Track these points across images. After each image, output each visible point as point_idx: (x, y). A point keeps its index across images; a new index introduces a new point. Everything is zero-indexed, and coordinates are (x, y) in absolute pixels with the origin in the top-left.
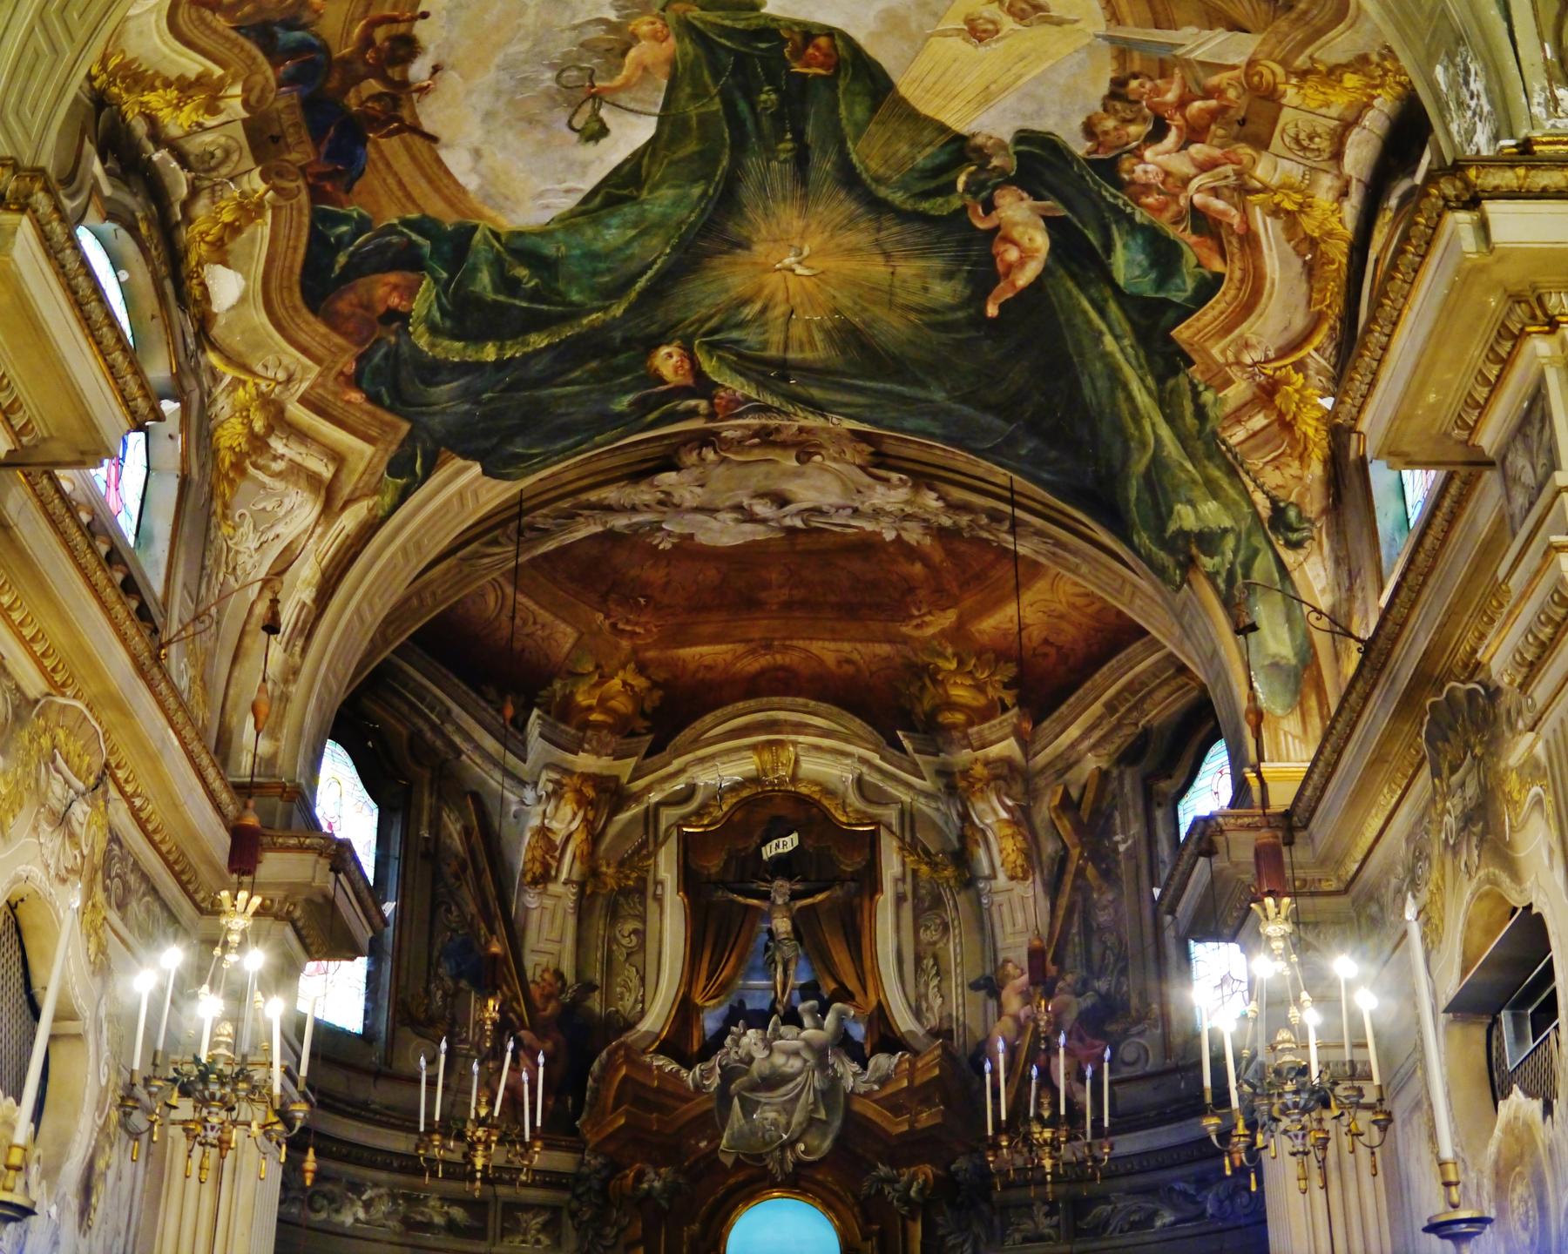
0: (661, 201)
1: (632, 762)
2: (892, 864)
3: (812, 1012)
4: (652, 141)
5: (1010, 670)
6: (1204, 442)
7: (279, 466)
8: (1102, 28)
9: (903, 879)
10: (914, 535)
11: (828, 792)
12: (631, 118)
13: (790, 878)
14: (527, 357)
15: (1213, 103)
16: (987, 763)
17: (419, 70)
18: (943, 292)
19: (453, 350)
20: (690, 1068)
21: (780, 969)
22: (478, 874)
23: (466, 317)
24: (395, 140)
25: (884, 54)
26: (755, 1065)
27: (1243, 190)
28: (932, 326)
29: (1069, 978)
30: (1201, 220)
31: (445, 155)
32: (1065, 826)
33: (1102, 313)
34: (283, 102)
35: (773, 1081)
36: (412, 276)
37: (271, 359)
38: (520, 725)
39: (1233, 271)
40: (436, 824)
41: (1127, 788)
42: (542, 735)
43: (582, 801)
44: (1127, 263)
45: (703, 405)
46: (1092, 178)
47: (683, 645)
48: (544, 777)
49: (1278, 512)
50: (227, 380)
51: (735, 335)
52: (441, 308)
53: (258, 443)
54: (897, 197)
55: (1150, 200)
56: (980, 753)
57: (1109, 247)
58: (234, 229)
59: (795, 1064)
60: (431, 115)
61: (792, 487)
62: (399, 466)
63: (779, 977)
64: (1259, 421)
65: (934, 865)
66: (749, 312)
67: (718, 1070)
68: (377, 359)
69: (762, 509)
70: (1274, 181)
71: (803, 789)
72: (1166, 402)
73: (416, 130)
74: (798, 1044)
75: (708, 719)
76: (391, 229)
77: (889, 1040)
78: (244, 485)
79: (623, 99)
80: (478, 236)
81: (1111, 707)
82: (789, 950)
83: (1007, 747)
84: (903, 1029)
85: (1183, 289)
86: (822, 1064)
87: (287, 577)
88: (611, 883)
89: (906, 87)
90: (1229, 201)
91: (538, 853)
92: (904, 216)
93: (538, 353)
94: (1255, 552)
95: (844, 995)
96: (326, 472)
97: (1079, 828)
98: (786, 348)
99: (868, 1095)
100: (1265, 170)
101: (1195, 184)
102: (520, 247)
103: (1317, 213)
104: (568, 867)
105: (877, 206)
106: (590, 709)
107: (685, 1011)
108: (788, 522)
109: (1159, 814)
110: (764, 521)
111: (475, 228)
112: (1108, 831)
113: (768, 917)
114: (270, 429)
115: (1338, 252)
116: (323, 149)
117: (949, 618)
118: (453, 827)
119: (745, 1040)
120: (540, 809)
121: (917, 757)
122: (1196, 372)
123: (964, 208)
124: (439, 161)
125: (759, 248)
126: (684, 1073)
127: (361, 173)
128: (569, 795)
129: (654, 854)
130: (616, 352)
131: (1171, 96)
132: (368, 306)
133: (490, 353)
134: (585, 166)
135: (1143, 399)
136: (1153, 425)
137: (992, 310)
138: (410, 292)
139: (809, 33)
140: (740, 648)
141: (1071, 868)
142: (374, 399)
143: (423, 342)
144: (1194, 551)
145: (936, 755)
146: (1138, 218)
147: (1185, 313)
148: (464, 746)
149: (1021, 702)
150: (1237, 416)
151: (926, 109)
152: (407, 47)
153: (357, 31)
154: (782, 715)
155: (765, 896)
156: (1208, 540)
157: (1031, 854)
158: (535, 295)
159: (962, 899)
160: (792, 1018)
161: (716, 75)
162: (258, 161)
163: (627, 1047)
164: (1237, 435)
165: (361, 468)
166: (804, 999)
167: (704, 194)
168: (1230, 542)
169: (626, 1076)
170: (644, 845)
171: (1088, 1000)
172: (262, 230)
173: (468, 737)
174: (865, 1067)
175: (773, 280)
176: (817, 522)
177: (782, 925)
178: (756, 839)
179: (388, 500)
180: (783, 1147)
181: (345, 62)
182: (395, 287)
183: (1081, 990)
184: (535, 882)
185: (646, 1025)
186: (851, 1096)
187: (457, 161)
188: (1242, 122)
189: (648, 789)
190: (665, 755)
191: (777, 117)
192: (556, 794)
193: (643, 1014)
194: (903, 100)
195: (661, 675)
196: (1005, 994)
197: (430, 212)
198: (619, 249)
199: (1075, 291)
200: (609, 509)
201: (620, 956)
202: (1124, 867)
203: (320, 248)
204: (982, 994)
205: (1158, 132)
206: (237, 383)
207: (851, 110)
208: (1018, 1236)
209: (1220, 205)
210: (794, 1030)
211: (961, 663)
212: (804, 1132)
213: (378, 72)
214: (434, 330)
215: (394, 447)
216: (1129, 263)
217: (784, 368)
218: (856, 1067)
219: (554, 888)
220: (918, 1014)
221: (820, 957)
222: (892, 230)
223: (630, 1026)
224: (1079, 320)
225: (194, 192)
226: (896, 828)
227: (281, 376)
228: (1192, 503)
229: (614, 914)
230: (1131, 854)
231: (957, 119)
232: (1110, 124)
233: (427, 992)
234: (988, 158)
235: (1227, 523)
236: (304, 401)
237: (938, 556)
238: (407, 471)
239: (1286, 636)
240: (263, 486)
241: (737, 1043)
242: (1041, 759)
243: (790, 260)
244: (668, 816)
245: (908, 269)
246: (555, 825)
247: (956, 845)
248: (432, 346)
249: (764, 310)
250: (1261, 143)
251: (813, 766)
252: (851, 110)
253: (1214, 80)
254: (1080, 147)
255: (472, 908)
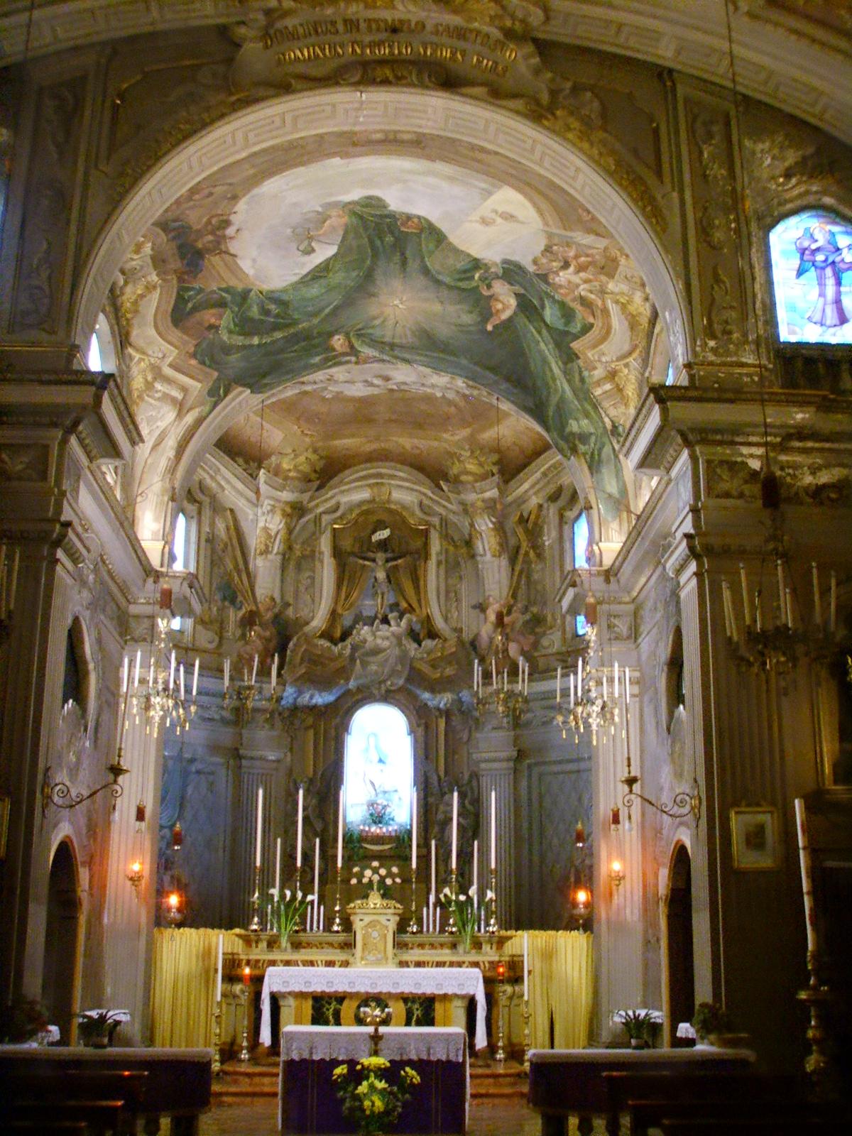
0: (337, 277)
1: (309, 494)
2: (436, 545)
3: (395, 618)
4: (335, 255)
5: (495, 457)
6: (583, 392)
7: (158, 395)
8: (542, 227)
9: (441, 553)
10: (451, 395)
11: (404, 507)
12: (327, 246)
13: (386, 551)
14: (273, 342)
15: (589, 259)
16: (483, 501)
17: (230, 231)
18: (468, 319)
19: (239, 340)
20: (336, 644)
21: (380, 596)
22: (233, 550)
23: (246, 326)
24: (217, 257)
25: (443, 226)
26: (367, 644)
27: (603, 292)
28: (462, 331)
29: (519, 605)
30: (583, 301)
31: (239, 262)
32: (520, 531)
33: (539, 333)
34: (169, 249)
35: (376, 651)
36: (221, 310)
37: (156, 349)
38: (254, 477)
39: (598, 324)
40: (212, 525)
41: (551, 514)
42: (265, 482)
43: (285, 515)
44: (550, 314)
45: (354, 359)
46: (535, 280)
47: (336, 439)
48: (266, 502)
49: (615, 427)
50: (136, 359)
51: (370, 331)
52: (236, 325)
53: (149, 386)
54: (447, 280)
55: (562, 291)
56: (480, 496)
57: (543, 307)
58: (142, 296)
59: (386, 644)
60: (233, 247)
61: (392, 373)
62: (213, 392)
63: (379, 600)
64: (608, 387)
65: (456, 546)
66: (377, 322)
67: (349, 646)
68: (204, 345)
69: (376, 381)
70: (616, 290)
71: (393, 507)
72: (566, 373)
73: (227, 252)
74: (388, 634)
75: (347, 472)
76: (214, 292)
77: (433, 635)
78: (143, 405)
79: (321, 238)
80: (252, 293)
81: (545, 474)
82: (385, 587)
83: (493, 493)
84: (439, 627)
85: (576, 327)
86: (400, 644)
87: (162, 445)
88: (298, 553)
89: (454, 239)
90: (597, 295)
91: (263, 539)
92: (450, 288)
93: (278, 339)
94: (603, 445)
95: (411, 609)
96: (178, 395)
97: (527, 531)
98: (393, 338)
99: (422, 659)
100: (611, 286)
101: (582, 287)
102: (272, 297)
103: (636, 305)
104: (277, 547)
105: (438, 283)
106: (290, 470)
107: (334, 615)
108: (390, 387)
109: (566, 527)
110: (378, 386)
111: (250, 290)
112: (540, 534)
113: (373, 570)
114: (155, 379)
115: (644, 322)
116: (185, 262)
117: (466, 432)
118: (221, 526)
119: (363, 632)
120: (264, 518)
121: (450, 494)
122: (580, 362)
123: (477, 287)
124: (237, 264)
125: (383, 298)
126: (333, 647)
127: (201, 271)
128: (279, 512)
129: (318, 538)
130: (314, 338)
131: (572, 254)
132: (200, 324)
133: (256, 341)
134: (304, 264)
135: (556, 371)
136: (561, 383)
137: (490, 328)
138: (220, 317)
139: (409, 217)
140: (363, 440)
141: (522, 552)
142: (203, 363)
143: (225, 337)
144: (577, 442)
145: (459, 493)
146: (556, 297)
147: (576, 337)
148: (226, 486)
149: (502, 472)
150: (598, 383)
151: (462, 248)
152: (227, 223)
153: (205, 220)
154: (384, 471)
155: (374, 560)
156: (584, 438)
157: (503, 545)
158: (277, 316)
159: (469, 564)
160: (385, 621)
161: (366, 229)
162: (155, 267)
163: (306, 635)
164: (598, 392)
165: (196, 393)
166: (392, 611)
167: (358, 275)
168: (593, 439)
169: (306, 650)
170: (314, 533)
171: (527, 617)
172: (156, 295)
173: (228, 482)
174: (420, 645)
175: (388, 311)
176: (403, 387)
177: (381, 575)
178: (369, 531)
179: (207, 408)
180: (380, 683)
181: (199, 231)
182: (214, 315)
183: (526, 609)
184: (261, 554)
185: (315, 623)
186: (412, 659)
187: (246, 265)
188: (603, 268)
189: (317, 506)
190: (323, 491)
191: (394, 246)
192: (272, 511)
193: (313, 618)
194: (450, 244)
195: (324, 453)
196: (488, 612)
197: (231, 284)
198: (317, 297)
199: (527, 323)
200: (303, 383)
201: (302, 589)
202: (547, 553)
203: (181, 300)
204: (478, 610)
205: (566, 265)
206: (141, 360)
207: (427, 245)
208: (490, 727)
209: (593, 296)
210: (386, 626)
211: (472, 452)
212: (390, 676)
213: (212, 233)
214: (230, 332)
215: (210, 384)
216: (551, 315)
217: (392, 346)
218: (415, 645)
219: (270, 557)
220: (446, 619)
221: (401, 591)
222: (445, 293)
223: (307, 623)
224: (529, 335)
225: (126, 283)
226: (438, 527)
227: (160, 355)
228: (577, 419)
229: (299, 568)
230: (551, 547)
231: (475, 253)
232: (544, 261)
233: (210, 608)
234: (489, 268)
235: (592, 430)
236: (170, 366)
237: (462, 404)
238: (217, 394)
239: (614, 482)
240: (151, 405)
241: (358, 633)
242: (510, 499)
243: (396, 302)
244: (325, 519)
245: (452, 309)
246: (271, 526)
247: (467, 537)
248: (229, 338)
249: (384, 321)
250: (611, 276)
251: (397, 495)
252: (427, 245)
253: (590, 252)
254: (531, 268)
255: (230, 566)
